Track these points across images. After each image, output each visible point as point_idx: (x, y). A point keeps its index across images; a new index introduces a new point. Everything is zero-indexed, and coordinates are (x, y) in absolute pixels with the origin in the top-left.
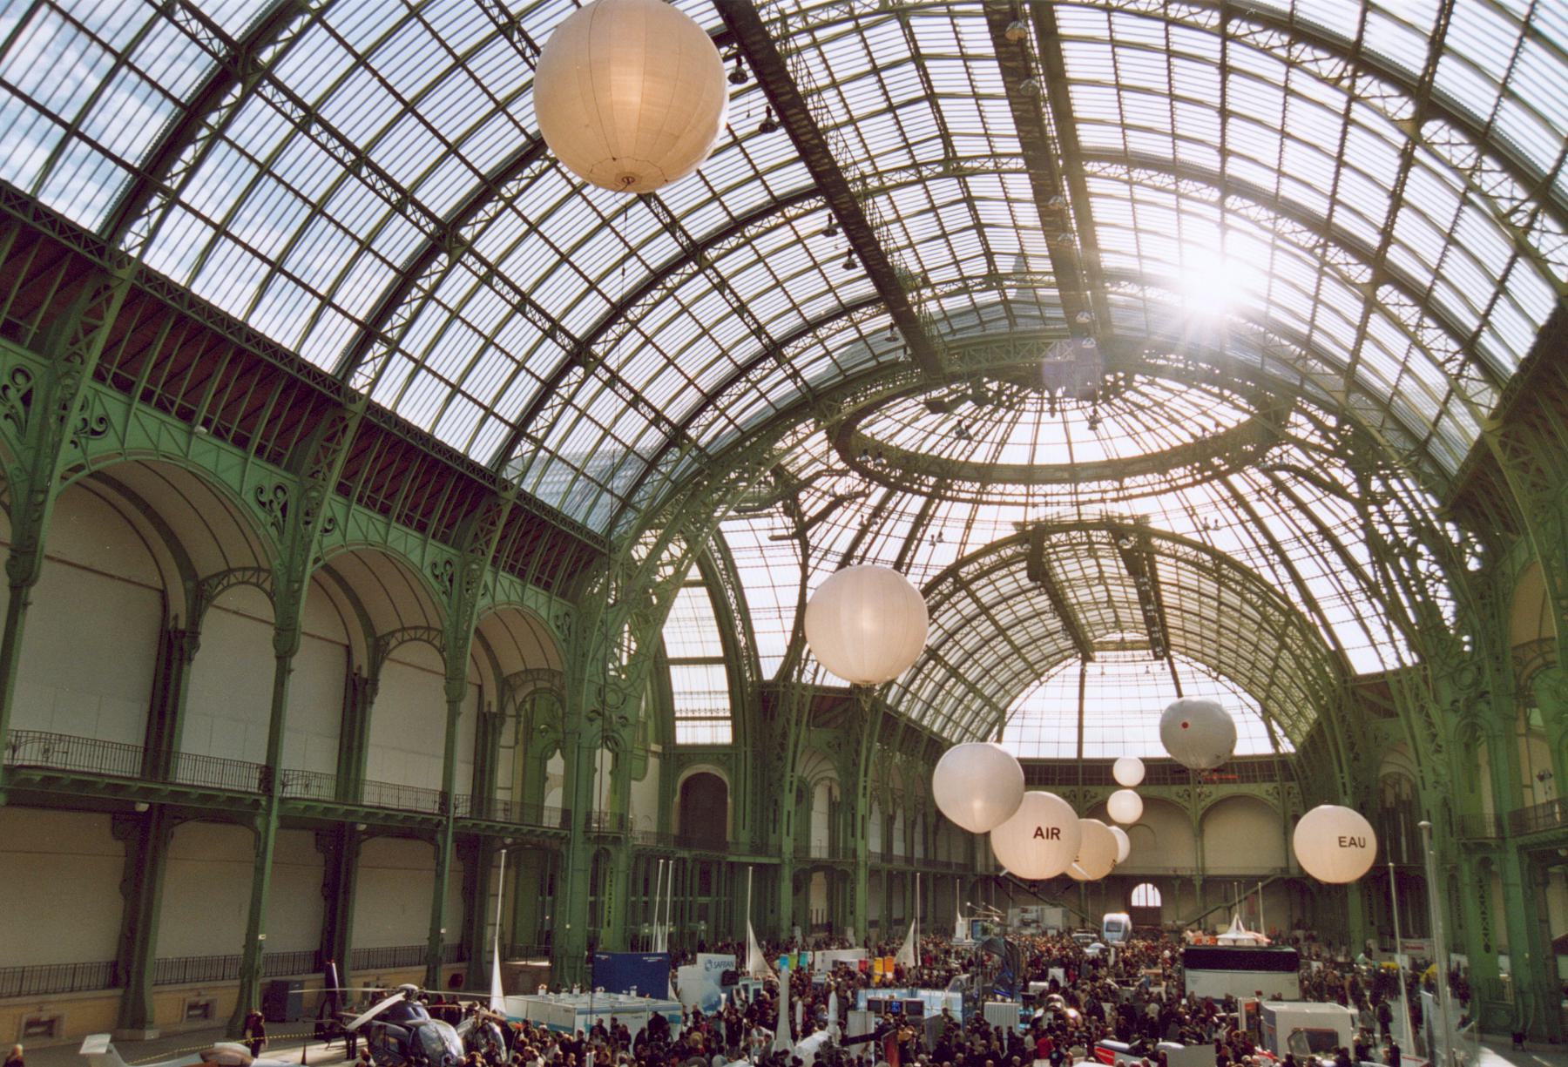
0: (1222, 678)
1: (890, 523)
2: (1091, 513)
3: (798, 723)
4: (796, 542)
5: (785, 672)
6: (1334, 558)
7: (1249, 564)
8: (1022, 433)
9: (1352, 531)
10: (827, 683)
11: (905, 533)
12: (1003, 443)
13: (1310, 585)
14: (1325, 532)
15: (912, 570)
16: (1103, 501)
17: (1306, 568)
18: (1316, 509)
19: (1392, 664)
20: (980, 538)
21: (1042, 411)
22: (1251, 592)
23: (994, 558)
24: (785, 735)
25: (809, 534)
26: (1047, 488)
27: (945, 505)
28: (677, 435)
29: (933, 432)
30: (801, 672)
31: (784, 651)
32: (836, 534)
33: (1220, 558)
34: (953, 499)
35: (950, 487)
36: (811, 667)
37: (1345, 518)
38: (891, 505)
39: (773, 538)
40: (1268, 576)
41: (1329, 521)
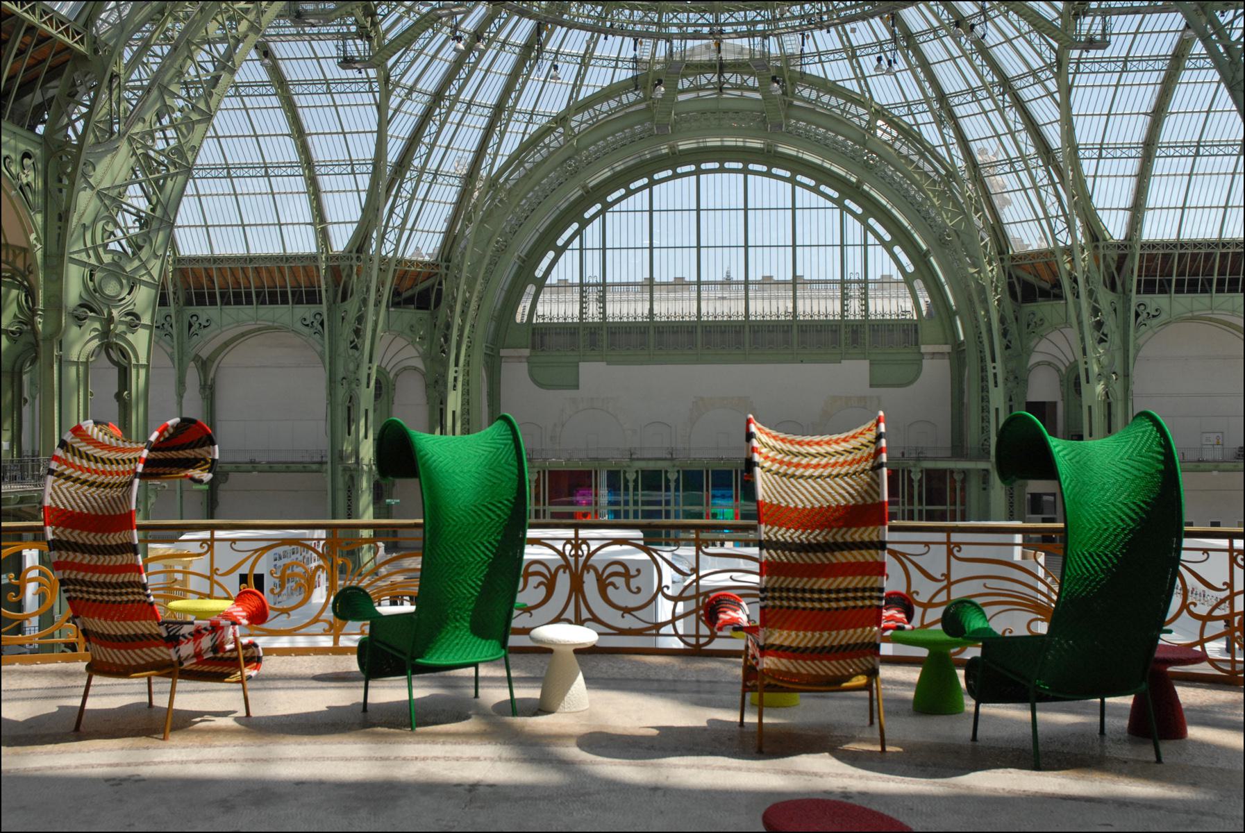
1: (490, 54)
2: (736, 47)
3: (378, 303)
4: (372, 73)
5: (360, 243)
6: (1011, 114)
7: (909, 120)
9: (1042, 82)
10: (408, 256)
11: (507, 69)
14: (1006, 83)
16: (750, 34)
17: (974, 127)
18: (1004, 56)
19: (1064, 238)
20: (598, 78)
23: (613, 104)
24: (360, 319)
25: (390, 63)
27: (560, 31)
30: (382, 238)
31: (357, 215)
32: (425, 67)
33: (881, 112)
34: (571, 26)
35: (566, 10)
36: (392, 236)
37: (1036, 63)
40: (931, 134)
41: (1013, 67)
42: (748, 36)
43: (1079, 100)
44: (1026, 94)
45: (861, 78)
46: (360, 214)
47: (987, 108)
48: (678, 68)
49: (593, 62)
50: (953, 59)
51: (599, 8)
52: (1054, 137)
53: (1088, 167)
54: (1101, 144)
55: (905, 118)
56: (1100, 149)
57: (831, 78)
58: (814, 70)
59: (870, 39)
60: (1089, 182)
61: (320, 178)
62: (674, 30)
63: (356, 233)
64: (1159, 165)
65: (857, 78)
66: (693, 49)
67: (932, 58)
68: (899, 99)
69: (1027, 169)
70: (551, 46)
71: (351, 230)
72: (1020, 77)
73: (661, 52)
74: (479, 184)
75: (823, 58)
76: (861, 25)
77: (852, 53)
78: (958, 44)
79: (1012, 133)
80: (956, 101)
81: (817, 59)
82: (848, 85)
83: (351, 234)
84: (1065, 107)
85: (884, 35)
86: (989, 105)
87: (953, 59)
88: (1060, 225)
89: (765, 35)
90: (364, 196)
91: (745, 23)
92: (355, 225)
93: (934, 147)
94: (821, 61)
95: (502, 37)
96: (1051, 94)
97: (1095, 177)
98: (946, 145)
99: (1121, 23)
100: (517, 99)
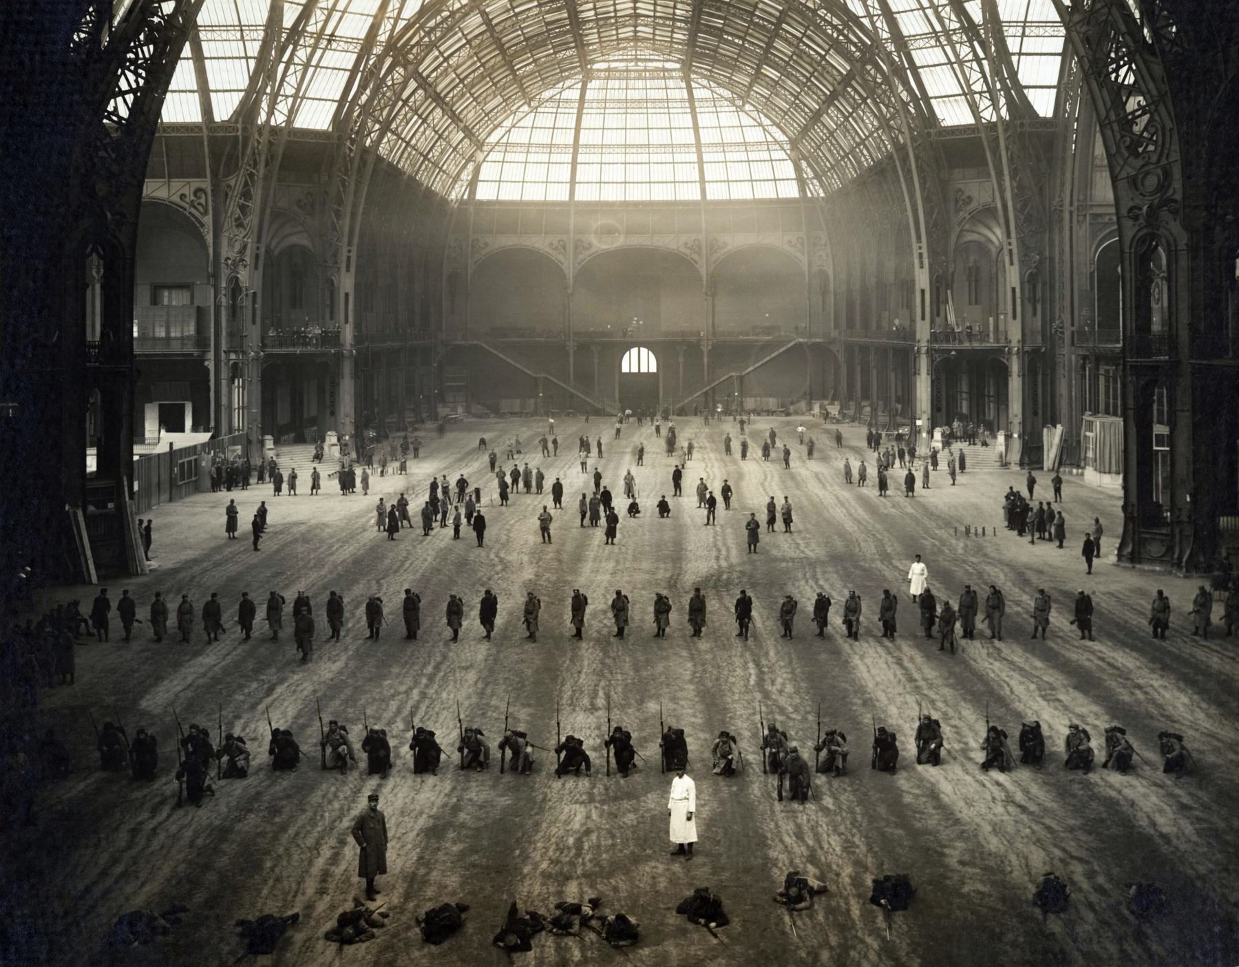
0: (748, 107)
5: (247, 109)
22: (834, 27)
24: (246, 195)
31: (244, 83)
46: (247, 81)
53: (1013, 45)
54: (1025, 22)
56: (1024, 27)
60: (1014, 59)
61: (204, 45)
63: (243, 103)
71: (237, 98)
74: (378, 50)
83: (236, 103)
88: (984, 103)
90: (252, 63)
92: (242, 94)
93: (858, 17)
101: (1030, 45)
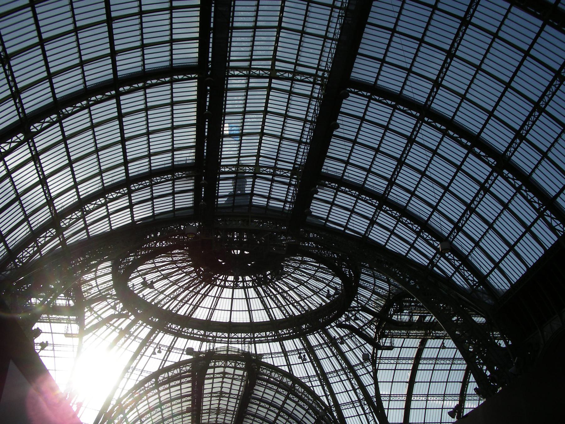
7: (309, 384)
8: (208, 302)
9: (365, 367)
12: (196, 307)
13: (338, 397)
14: (351, 368)
15: (135, 371)
17: (337, 388)
20: (174, 358)
21: (224, 287)
26: (214, 334)
28: (55, 221)
29: (162, 292)
38: (132, 330)
39: (67, 335)
40: (319, 391)
41: (353, 361)
42: (242, 344)
43: (381, 376)
44: (359, 373)
45: (289, 365)
47: (343, 379)
48: (211, 355)
49: (173, 350)
50: (328, 357)
51: (179, 327)
52: (371, 391)
53: (385, 405)
55: (307, 384)
57: (276, 365)
58: (269, 361)
59: (294, 348)
60: (386, 411)
62: (211, 338)
64: (413, 404)
65: (287, 365)
66: (217, 349)
67: (320, 357)
68: (305, 375)
69: (361, 405)
70: (156, 341)
72: (356, 365)
73: (203, 349)
75: (273, 356)
76: (290, 341)
77: (285, 353)
78: (331, 350)
79: (355, 390)
80: (330, 376)
81: (270, 356)
82: (283, 368)
84: (375, 378)
85: (300, 346)
86: (344, 377)
87: (328, 357)
89: (250, 343)
91: (241, 338)
94: (272, 357)
95: (135, 334)
96: (369, 373)
97: (388, 409)
98: (326, 396)
99: (398, 342)
100: (137, 363)
101: (393, 405)
